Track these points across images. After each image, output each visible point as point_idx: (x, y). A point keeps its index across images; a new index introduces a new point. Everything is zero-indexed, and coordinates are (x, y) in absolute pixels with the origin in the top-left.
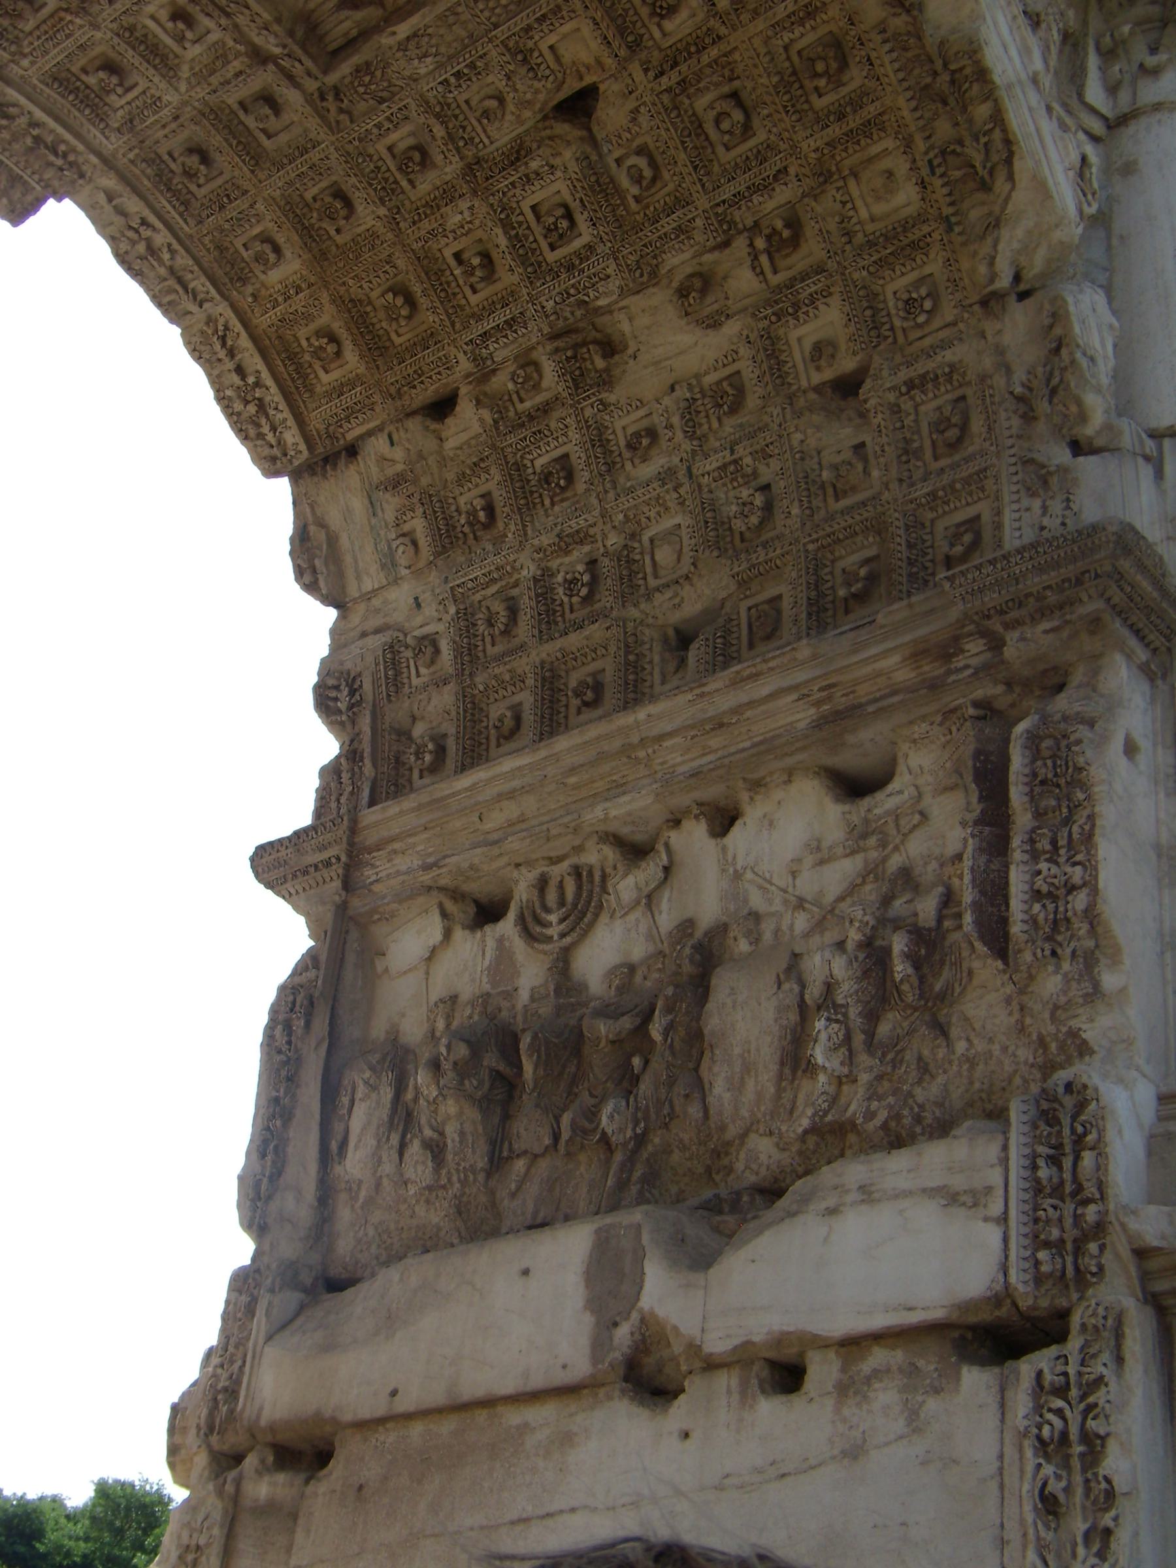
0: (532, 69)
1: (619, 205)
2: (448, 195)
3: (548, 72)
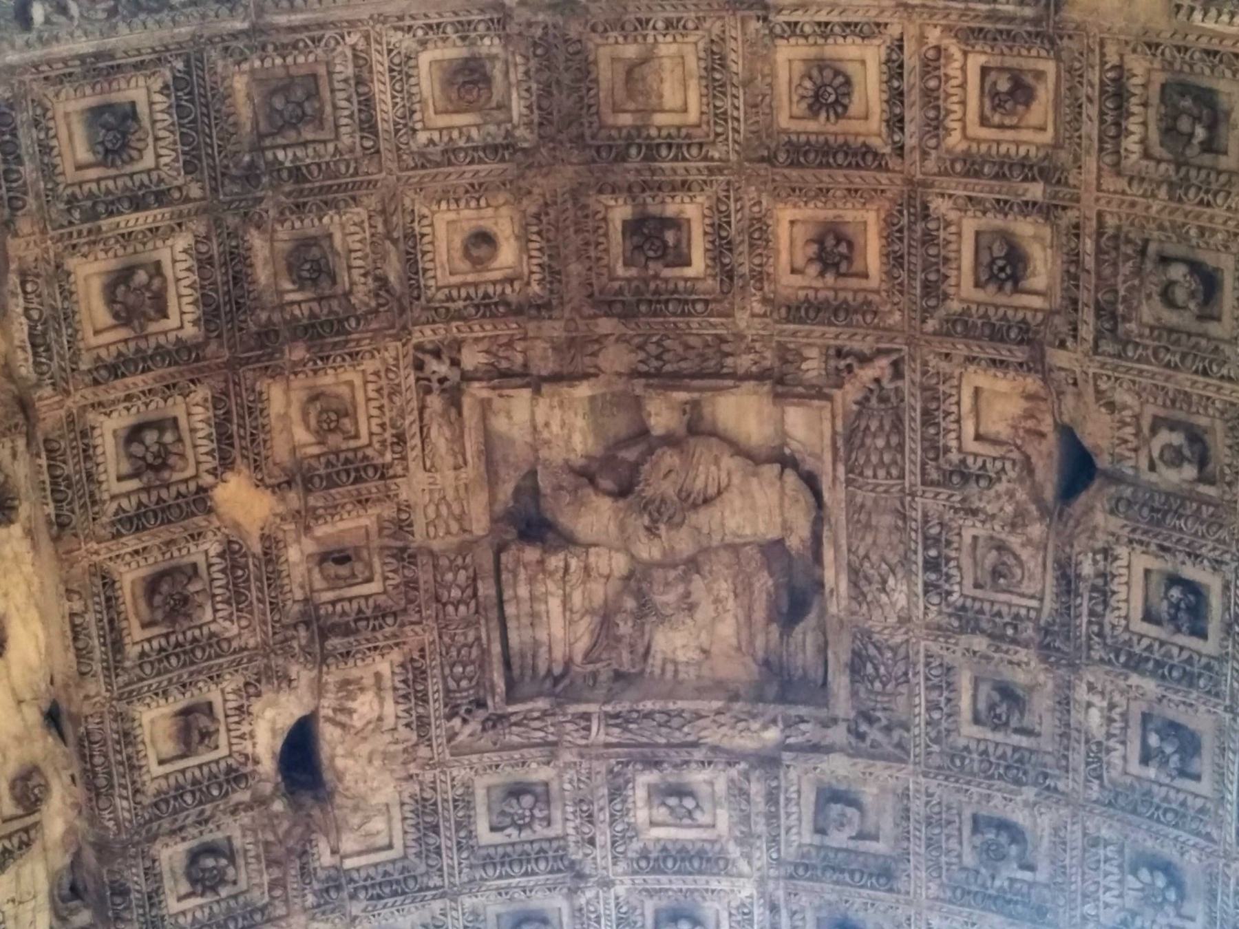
0: (978, 477)
1: (1199, 508)
2: (1065, 703)
3: (998, 464)
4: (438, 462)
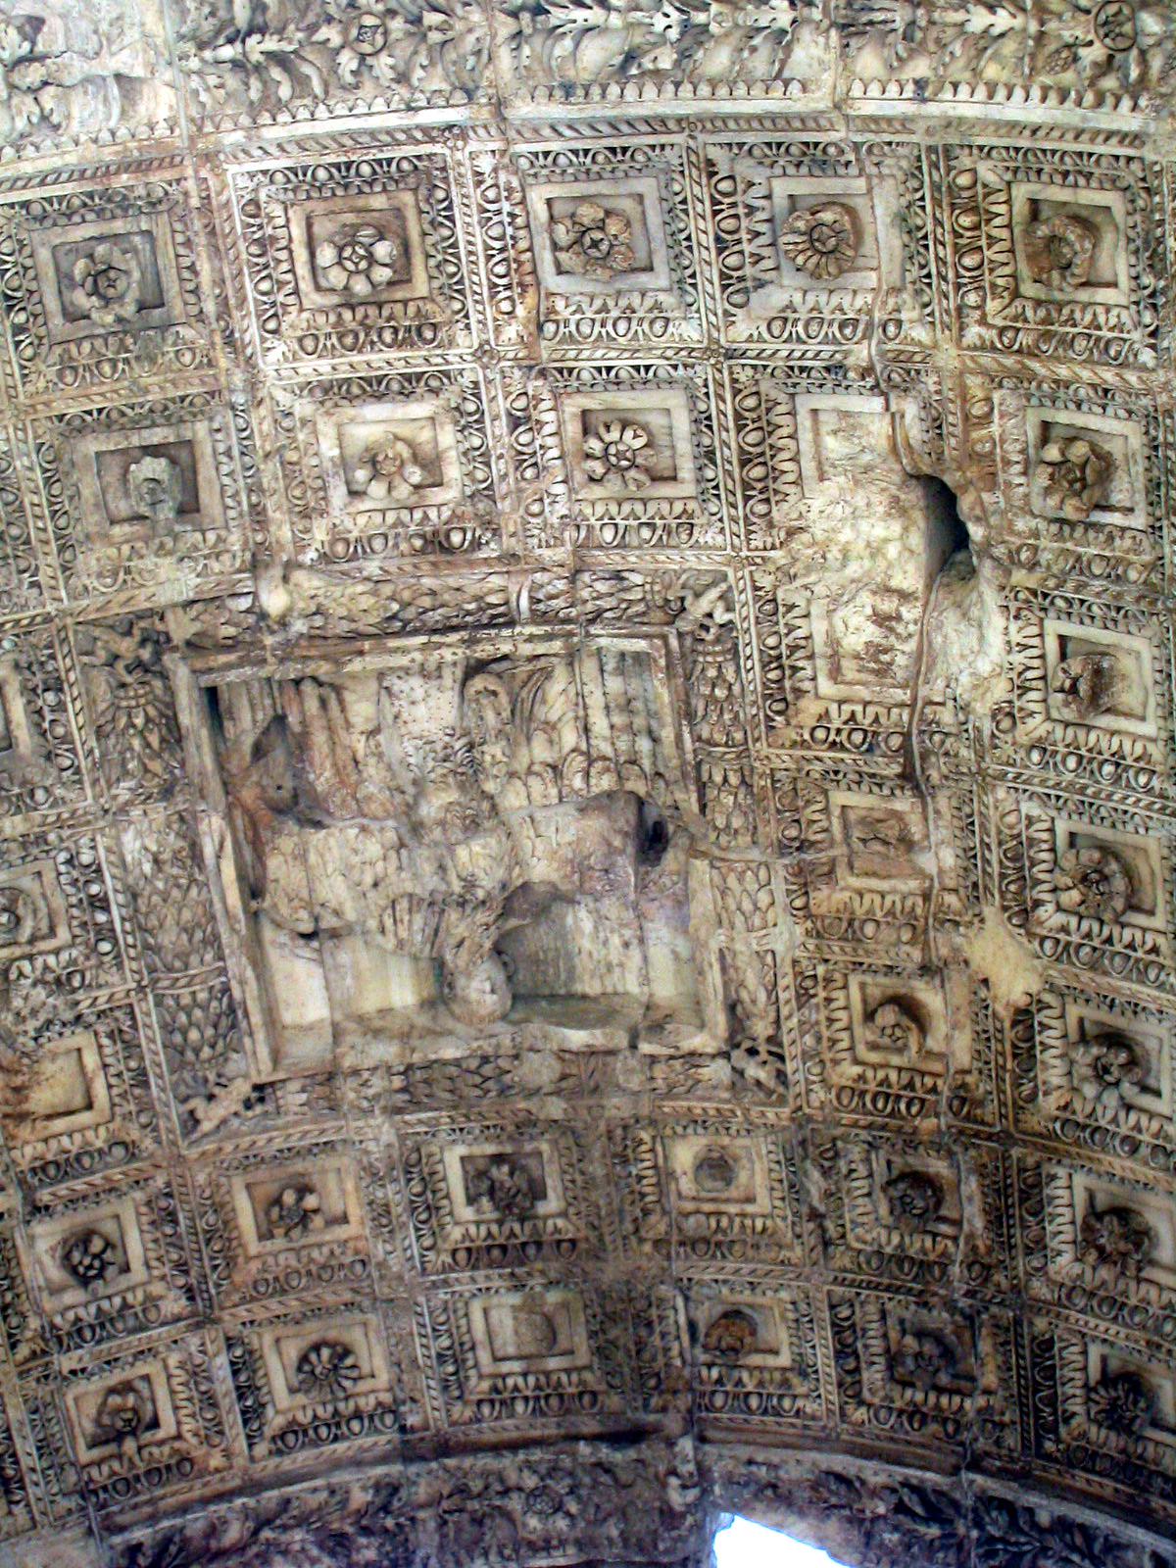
4: (757, 965)
